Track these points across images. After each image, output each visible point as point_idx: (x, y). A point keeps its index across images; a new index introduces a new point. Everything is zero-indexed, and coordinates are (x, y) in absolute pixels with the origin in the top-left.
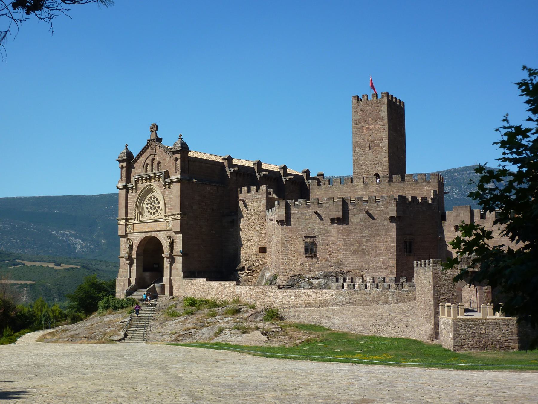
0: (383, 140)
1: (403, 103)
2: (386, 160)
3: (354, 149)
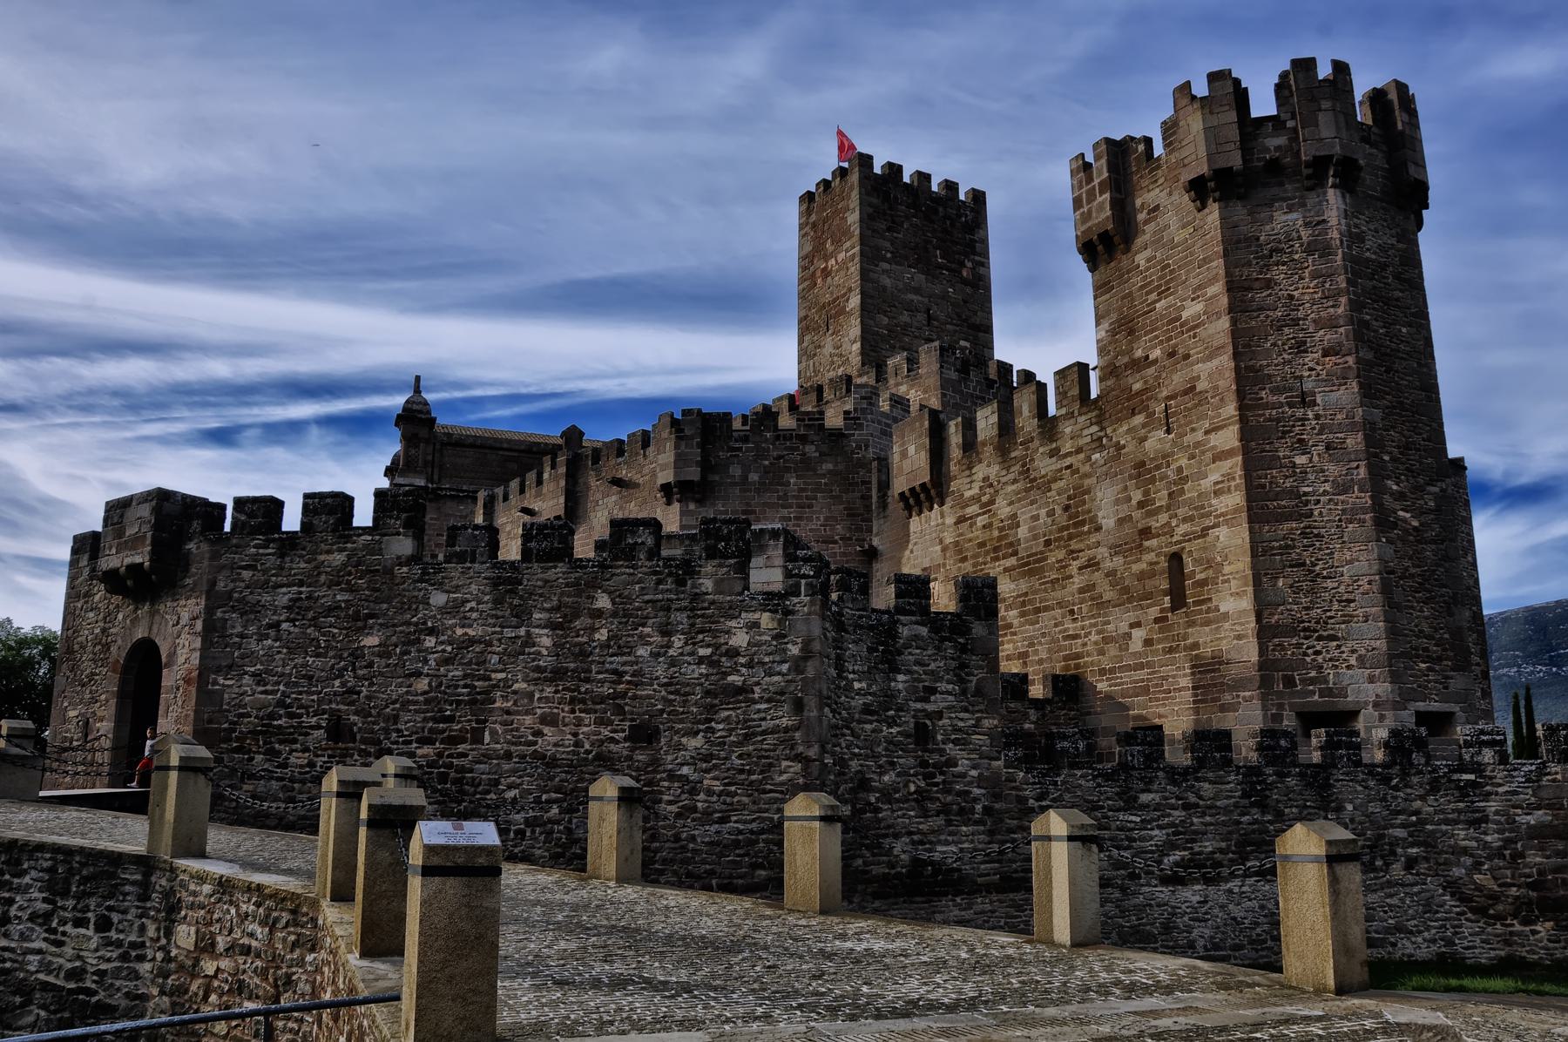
0: (850, 290)
1: (978, 197)
2: (857, 346)
3: (801, 342)
